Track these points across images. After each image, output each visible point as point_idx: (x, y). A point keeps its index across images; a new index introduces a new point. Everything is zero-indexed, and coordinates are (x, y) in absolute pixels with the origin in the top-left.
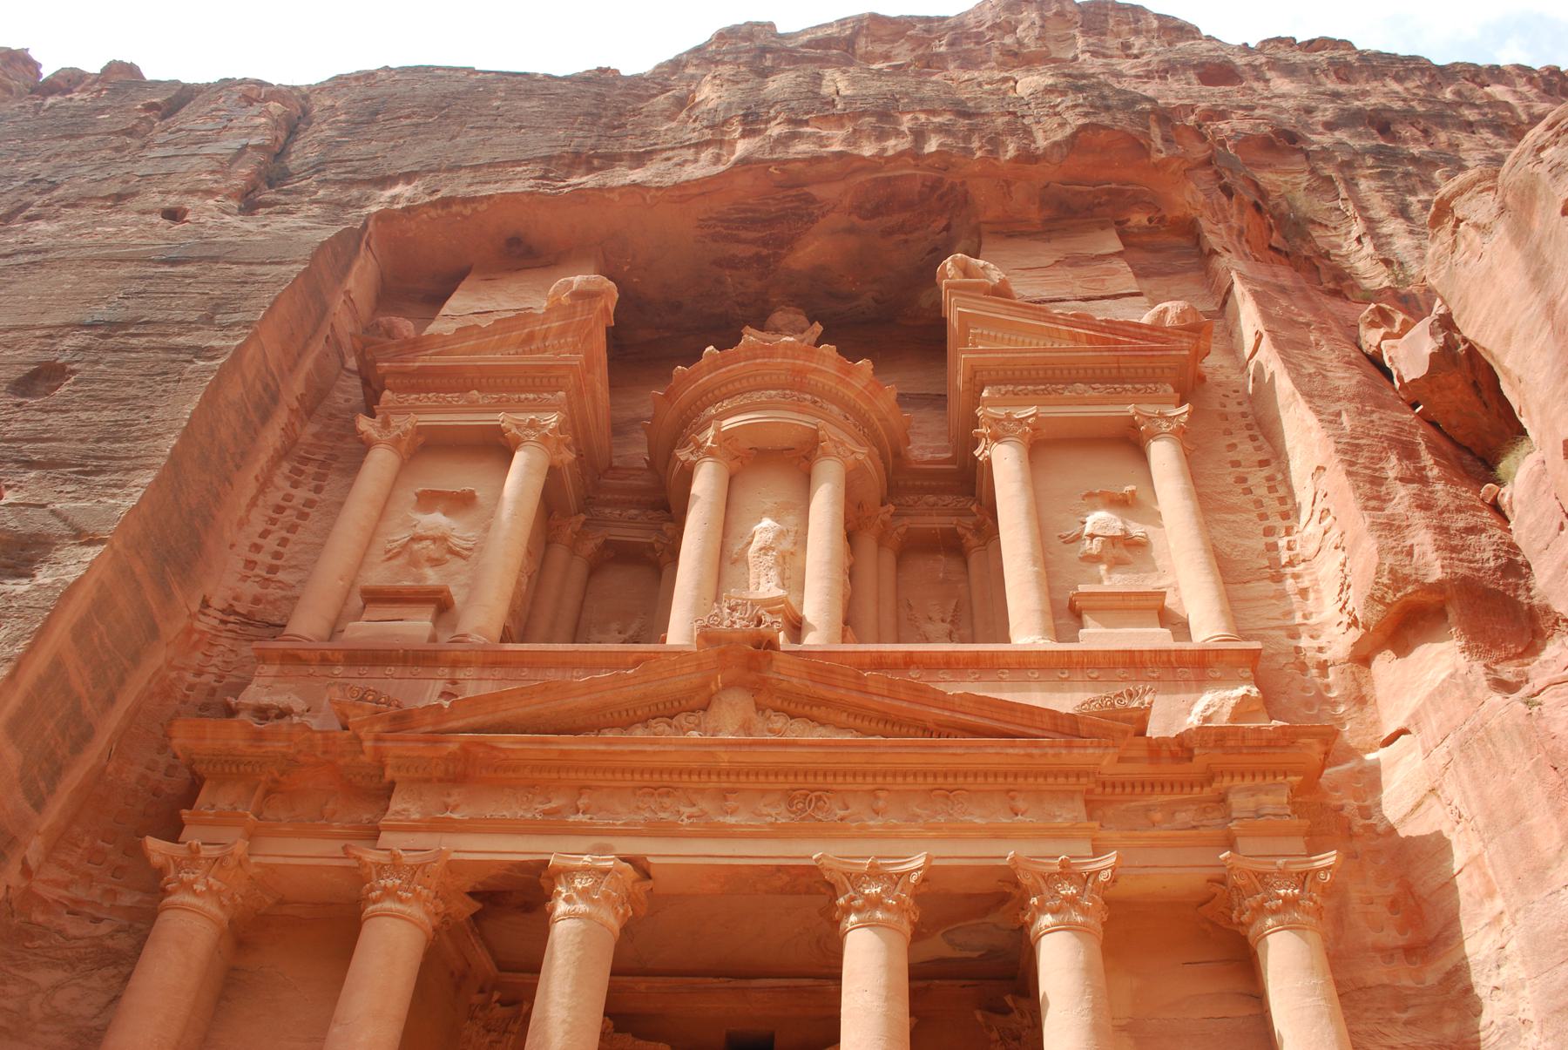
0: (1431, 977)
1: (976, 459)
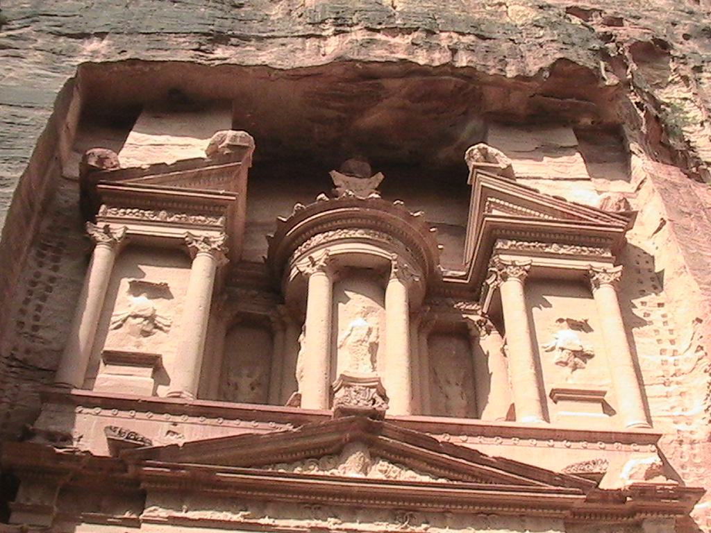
1: (488, 286)
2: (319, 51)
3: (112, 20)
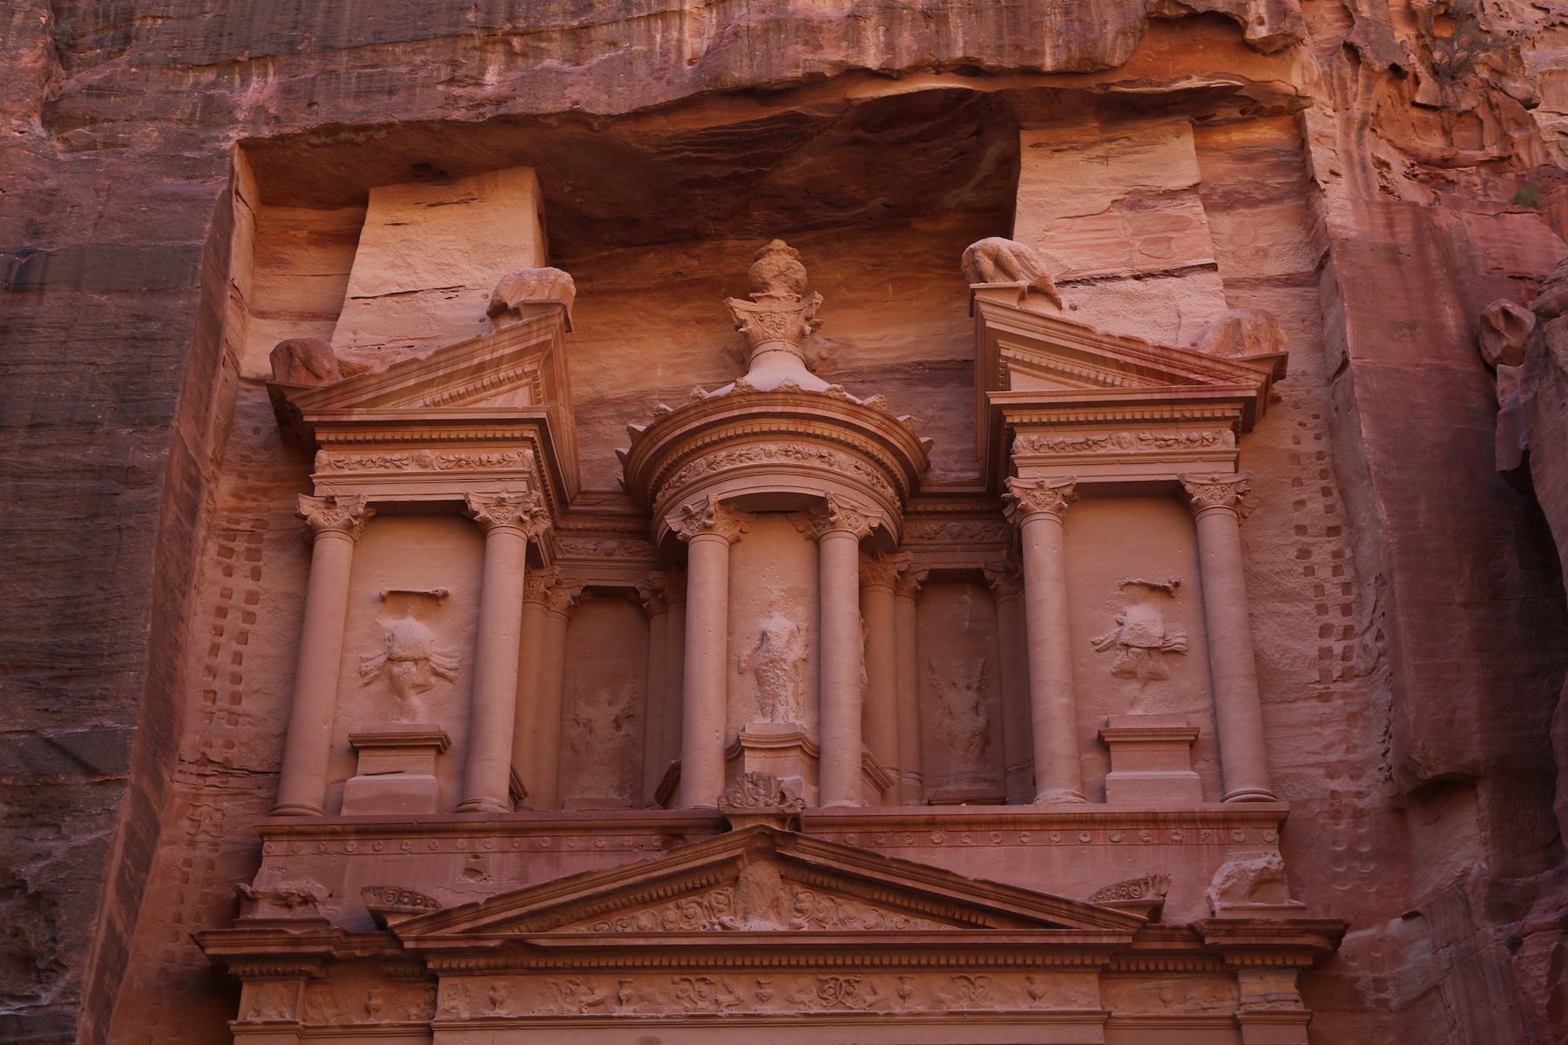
1: (1005, 520)
2: (680, 53)
3: (278, 18)
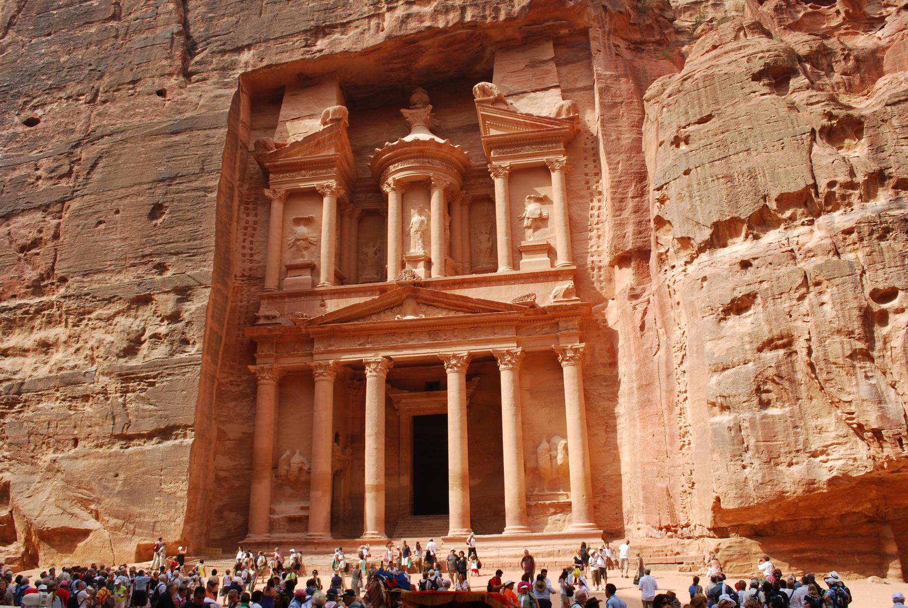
0: (615, 373)
2: (378, 27)
